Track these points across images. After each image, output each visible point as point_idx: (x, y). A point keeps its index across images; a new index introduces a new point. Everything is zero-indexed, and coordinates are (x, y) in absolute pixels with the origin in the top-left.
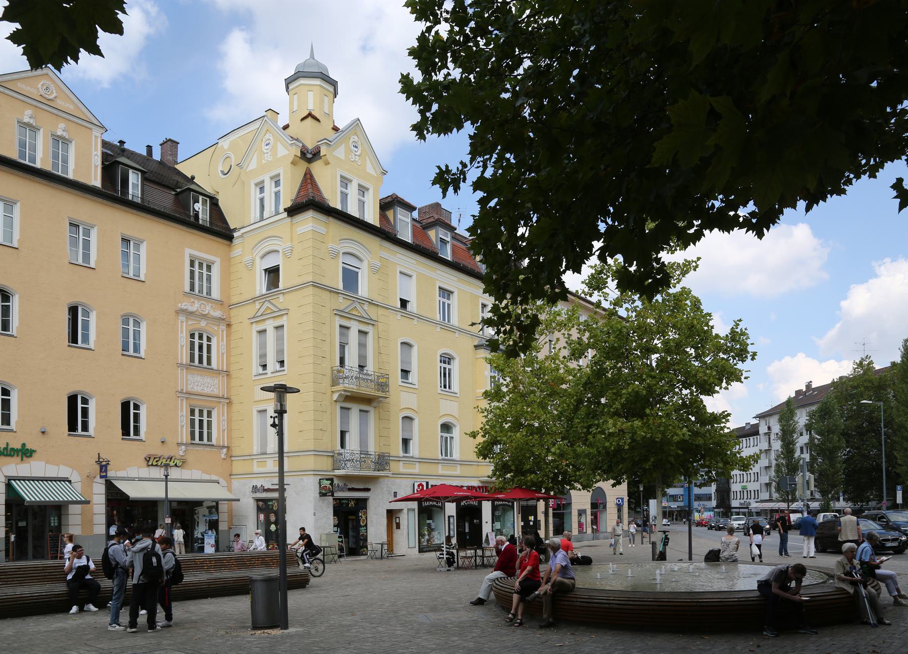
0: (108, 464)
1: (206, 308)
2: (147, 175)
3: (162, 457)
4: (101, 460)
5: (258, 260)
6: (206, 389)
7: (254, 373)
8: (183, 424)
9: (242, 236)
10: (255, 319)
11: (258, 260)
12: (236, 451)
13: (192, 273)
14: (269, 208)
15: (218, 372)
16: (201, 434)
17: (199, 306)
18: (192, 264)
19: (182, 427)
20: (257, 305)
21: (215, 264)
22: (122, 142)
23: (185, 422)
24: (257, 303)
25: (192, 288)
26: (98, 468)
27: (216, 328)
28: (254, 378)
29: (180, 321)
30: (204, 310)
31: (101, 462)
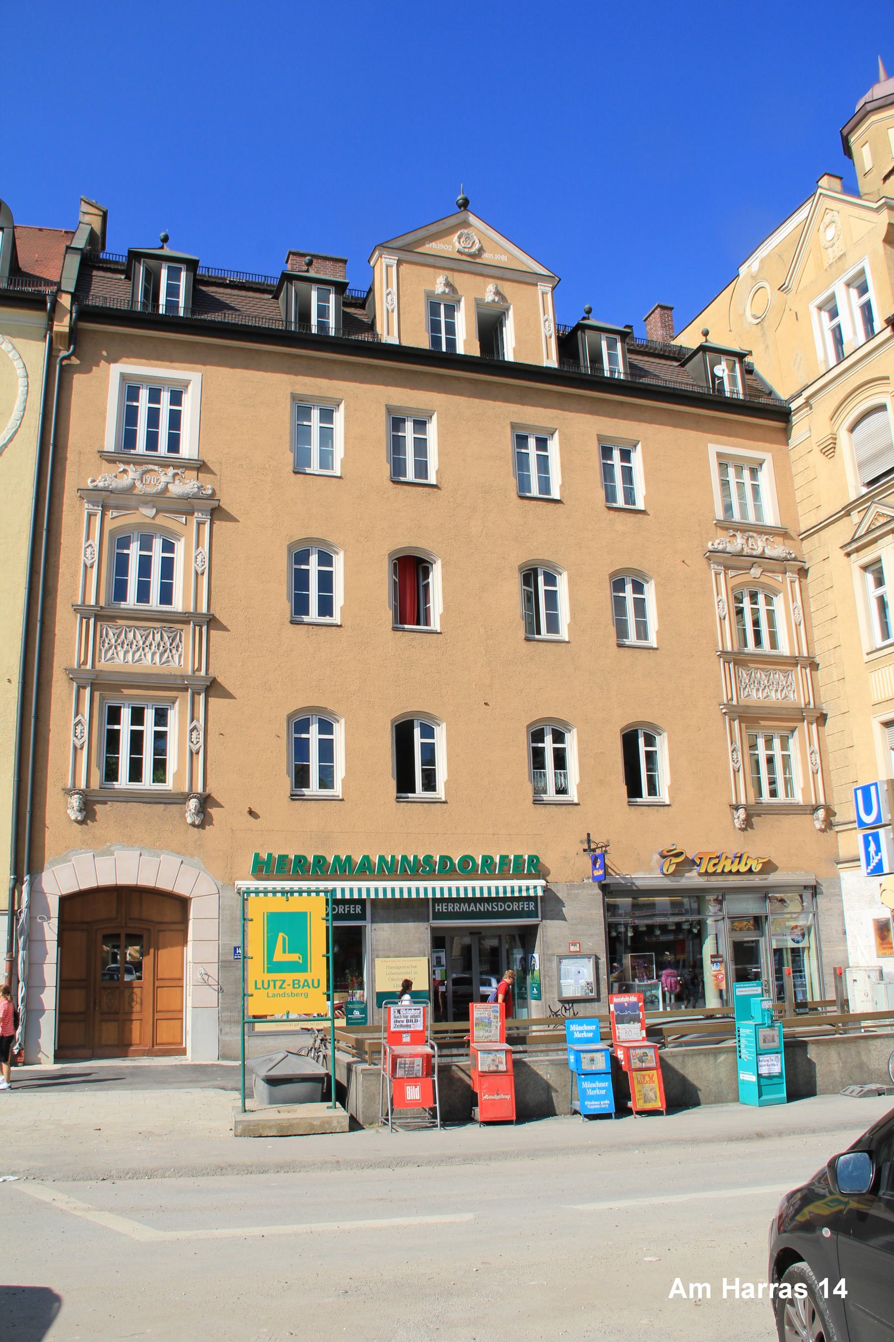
0: (606, 851)
1: (757, 544)
4: (593, 846)
5: (843, 435)
7: (866, 648)
8: (737, 766)
9: (807, 403)
10: (853, 547)
11: (843, 435)
14: (853, 335)
15: (793, 662)
17: (744, 541)
19: (736, 772)
20: (855, 517)
21: (764, 466)
23: (741, 762)
24: (854, 513)
26: (587, 860)
27: (780, 579)
28: (867, 658)
29: (713, 572)
31: (594, 850)
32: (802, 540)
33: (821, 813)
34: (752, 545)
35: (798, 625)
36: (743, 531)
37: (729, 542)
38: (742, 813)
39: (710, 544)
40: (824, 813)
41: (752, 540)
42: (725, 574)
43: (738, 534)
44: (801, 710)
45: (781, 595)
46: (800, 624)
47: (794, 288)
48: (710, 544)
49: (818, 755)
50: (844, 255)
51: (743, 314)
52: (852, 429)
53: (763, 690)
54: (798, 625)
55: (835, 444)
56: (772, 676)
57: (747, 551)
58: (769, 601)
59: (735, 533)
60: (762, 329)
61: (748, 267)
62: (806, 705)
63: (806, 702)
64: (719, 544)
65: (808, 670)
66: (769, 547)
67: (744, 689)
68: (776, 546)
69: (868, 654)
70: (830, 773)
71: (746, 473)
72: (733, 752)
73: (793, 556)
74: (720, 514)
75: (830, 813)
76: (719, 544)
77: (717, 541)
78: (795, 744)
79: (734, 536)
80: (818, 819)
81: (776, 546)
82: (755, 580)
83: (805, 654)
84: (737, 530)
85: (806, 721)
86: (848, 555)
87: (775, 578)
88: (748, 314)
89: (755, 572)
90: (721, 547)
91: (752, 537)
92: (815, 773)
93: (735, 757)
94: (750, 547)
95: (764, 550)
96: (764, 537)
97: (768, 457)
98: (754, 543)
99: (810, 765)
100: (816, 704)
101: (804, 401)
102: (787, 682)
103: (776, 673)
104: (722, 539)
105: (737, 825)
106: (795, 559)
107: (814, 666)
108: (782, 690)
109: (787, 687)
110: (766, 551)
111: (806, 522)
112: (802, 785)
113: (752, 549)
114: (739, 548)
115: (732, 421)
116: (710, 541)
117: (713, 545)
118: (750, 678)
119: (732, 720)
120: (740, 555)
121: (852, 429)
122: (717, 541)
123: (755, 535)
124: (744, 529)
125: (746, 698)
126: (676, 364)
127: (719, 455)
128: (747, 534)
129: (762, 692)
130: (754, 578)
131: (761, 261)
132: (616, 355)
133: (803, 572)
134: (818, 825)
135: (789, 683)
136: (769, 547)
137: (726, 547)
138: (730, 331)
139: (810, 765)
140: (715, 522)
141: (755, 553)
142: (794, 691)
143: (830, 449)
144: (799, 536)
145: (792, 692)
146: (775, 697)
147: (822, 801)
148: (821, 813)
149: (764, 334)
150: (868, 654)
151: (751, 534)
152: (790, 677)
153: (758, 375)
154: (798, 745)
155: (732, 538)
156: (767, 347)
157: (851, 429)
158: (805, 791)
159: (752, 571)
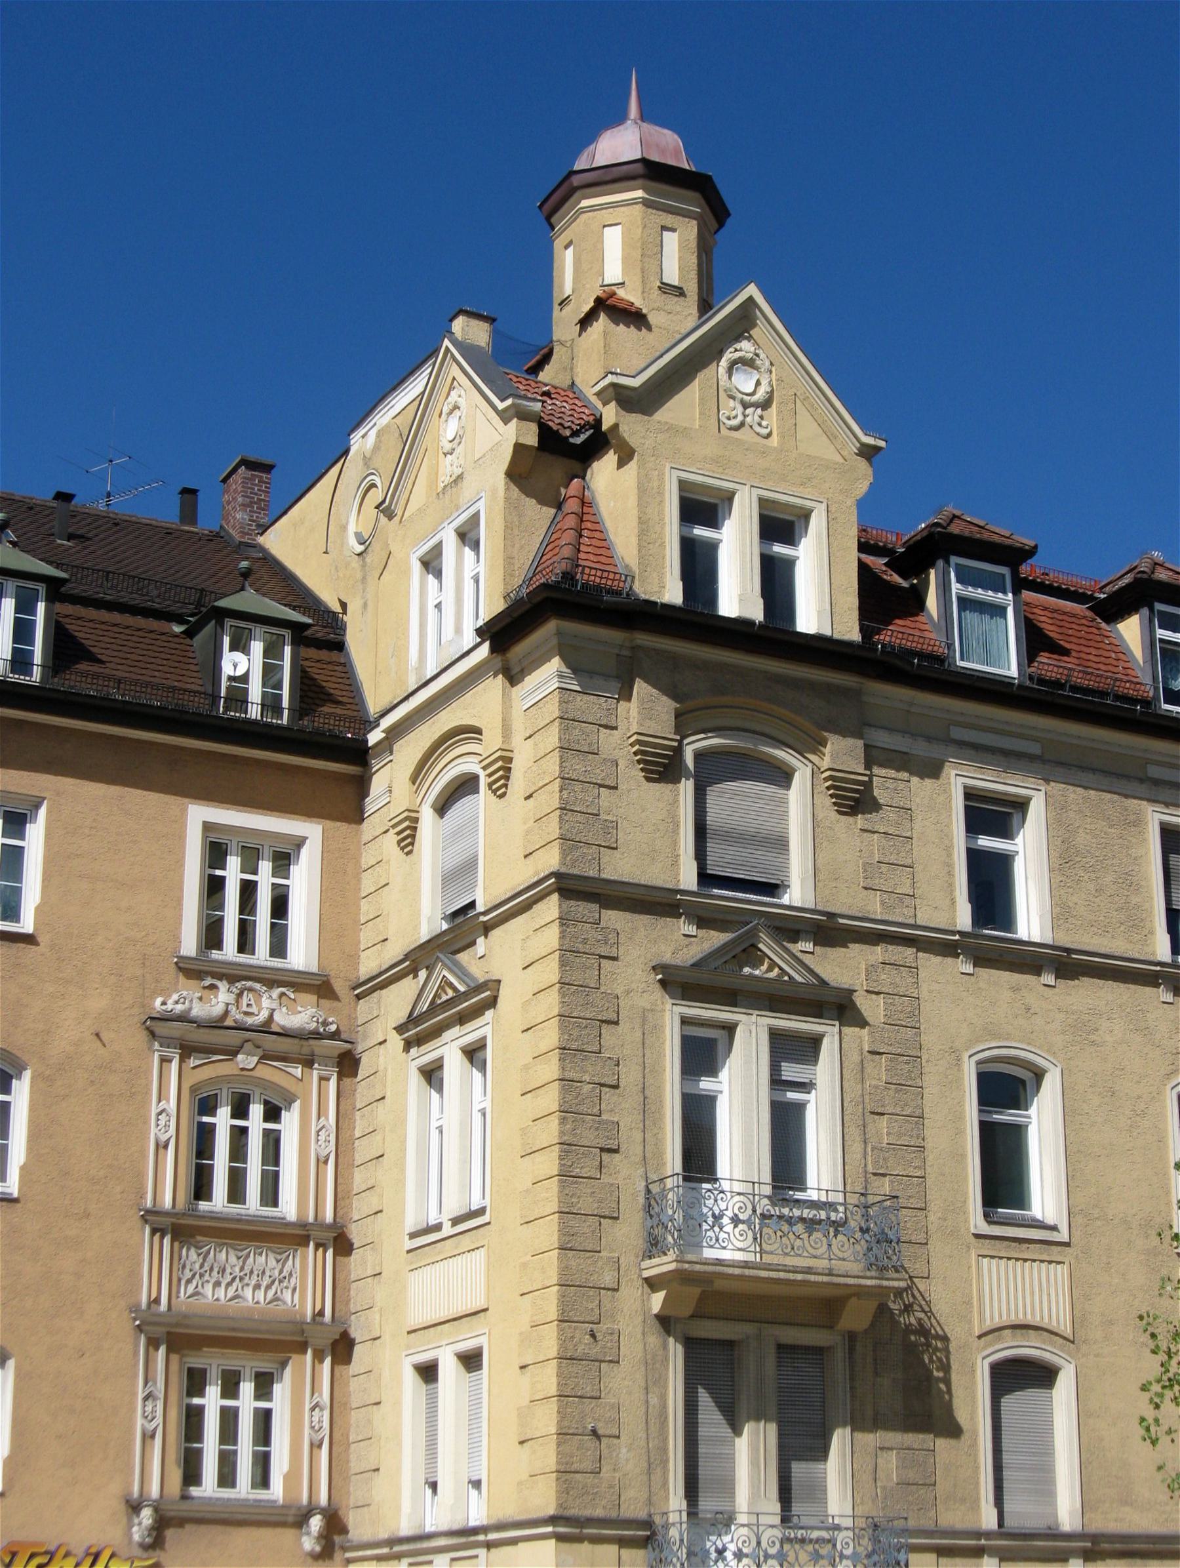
1: (259, 1004)
2: (308, 633)
3: (62, 1552)
5: (427, 815)
6: (287, 1295)
7: (410, 1226)
11: (427, 815)
12: (360, 1527)
13: (214, 887)
16: (227, 1463)
17: (231, 998)
18: (216, 853)
19: (148, 1437)
21: (304, 851)
22: (64, 497)
25: (212, 935)
30: (254, 1009)
32: (359, 997)
33: (316, 1523)
34: (248, 1005)
35: (322, 1162)
36: (232, 979)
37: (200, 999)
38: (146, 1516)
39: (159, 1001)
40: (319, 1524)
41: (251, 996)
42: (181, 1061)
43: (223, 986)
44: (299, 1326)
45: (296, 1105)
46: (326, 1162)
47: (399, 512)
48: (159, 1001)
49: (326, 1413)
50: (460, 477)
51: (344, 528)
52: (442, 808)
53: (229, 1284)
54: (322, 1162)
55: (415, 829)
56: (251, 1259)
57: (236, 1015)
58: (272, 1113)
59: (215, 982)
60: (364, 566)
61: (363, 437)
62: (314, 1316)
63: (316, 1312)
64: (177, 1002)
65: (330, 1254)
66: (284, 1009)
67: (189, 1281)
68: (300, 1009)
69: (413, 1236)
70: (347, 1449)
71: (265, 867)
72: (146, 1399)
73: (333, 1028)
74: (189, 944)
75: (335, 1525)
76: (177, 1002)
77: (175, 997)
78: (283, 1389)
79: (213, 987)
80: (308, 1534)
81: (300, 1009)
82: (244, 1073)
83: (329, 1217)
84: (220, 977)
85: (310, 1351)
86: (408, 1045)
87: (289, 1070)
88: (352, 528)
89: (246, 1060)
90: (179, 1008)
91: (250, 990)
92: (316, 1446)
93: (149, 1409)
94: (245, 1008)
95: (271, 1016)
96: (276, 992)
97: (311, 831)
98: (252, 1002)
99: (307, 1431)
100: (337, 1315)
101: (383, 735)
102: (281, 1272)
103: (261, 1254)
104: (185, 993)
105: (136, 1537)
106: (335, 1036)
107: (342, 1245)
108: (268, 1287)
109: (280, 1282)
110: (277, 1017)
111: (369, 964)
112: (286, 1468)
113: (246, 1014)
114: (218, 1010)
115: (246, 761)
116: (160, 995)
117: (164, 1003)
118: (204, 1260)
119: (153, 1343)
120: (217, 1024)
121: (442, 808)
122: (175, 997)
123: (257, 986)
124: (232, 975)
125: (191, 1299)
126: (178, 629)
127: (208, 827)
128: (239, 985)
129: (226, 1288)
130: (243, 1069)
131: (379, 435)
132: (33, 623)
133: (348, 1064)
134: (309, 1544)
135: (285, 1273)
136: (284, 1009)
137: (190, 1009)
138: (326, 552)
139: (307, 1431)
140: (176, 960)
141: (250, 1021)
142: (294, 1289)
143: (408, 838)
144: (354, 988)
145: (290, 1291)
146: (253, 1297)
147: (323, 1499)
148: (316, 1523)
149: (364, 579)
150: (413, 1236)
151: (249, 984)
152: (290, 1262)
153: (348, 656)
154: (288, 1393)
155: (207, 991)
156: (365, 605)
157: (439, 806)
158: (291, 1478)
159: (240, 1057)
